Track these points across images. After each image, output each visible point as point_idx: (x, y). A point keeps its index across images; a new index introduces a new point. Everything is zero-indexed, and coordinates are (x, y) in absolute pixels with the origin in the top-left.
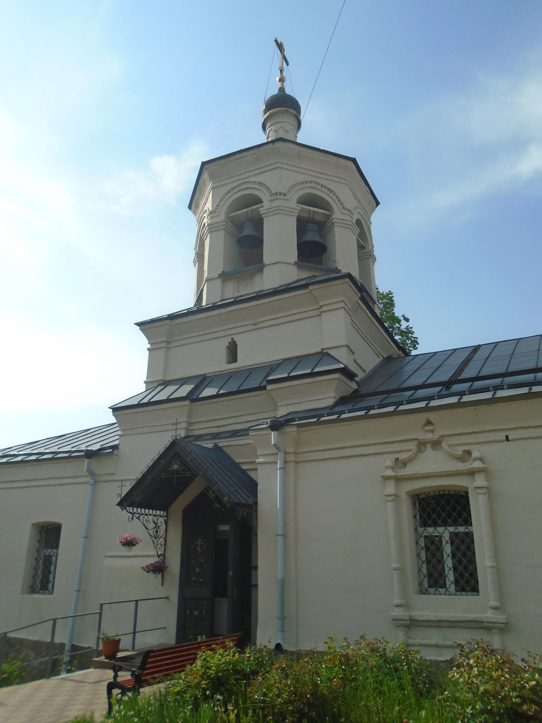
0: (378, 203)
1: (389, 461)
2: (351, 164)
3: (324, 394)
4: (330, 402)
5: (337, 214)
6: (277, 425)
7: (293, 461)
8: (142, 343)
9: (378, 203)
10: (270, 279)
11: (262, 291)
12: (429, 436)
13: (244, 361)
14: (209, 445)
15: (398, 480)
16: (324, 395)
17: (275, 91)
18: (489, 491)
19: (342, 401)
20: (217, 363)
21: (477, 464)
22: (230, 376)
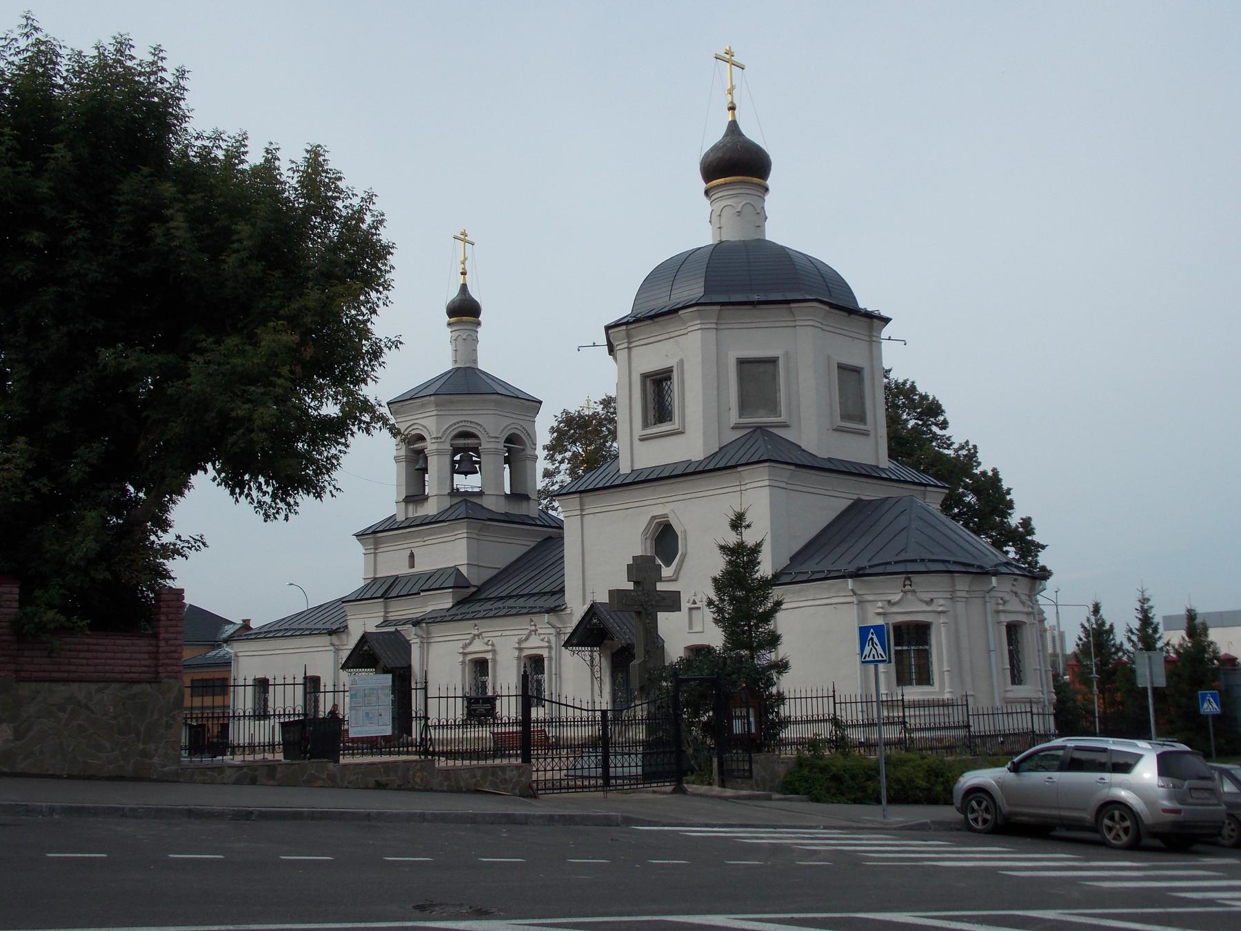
0: (541, 402)
1: (461, 644)
2: (495, 396)
3: (444, 602)
4: (450, 605)
5: (485, 445)
6: (416, 623)
7: (426, 642)
8: (358, 548)
9: (541, 402)
10: (431, 508)
11: (427, 516)
12: (476, 632)
13: (418, 568)
14: (392, 629)
15: (465, 654)
16: (444, 602)
17: (453, 294)
18: (494, 660)
19: (458, 604)
20: (403, 570)
21: (490, 648)
22: (409, 578)
